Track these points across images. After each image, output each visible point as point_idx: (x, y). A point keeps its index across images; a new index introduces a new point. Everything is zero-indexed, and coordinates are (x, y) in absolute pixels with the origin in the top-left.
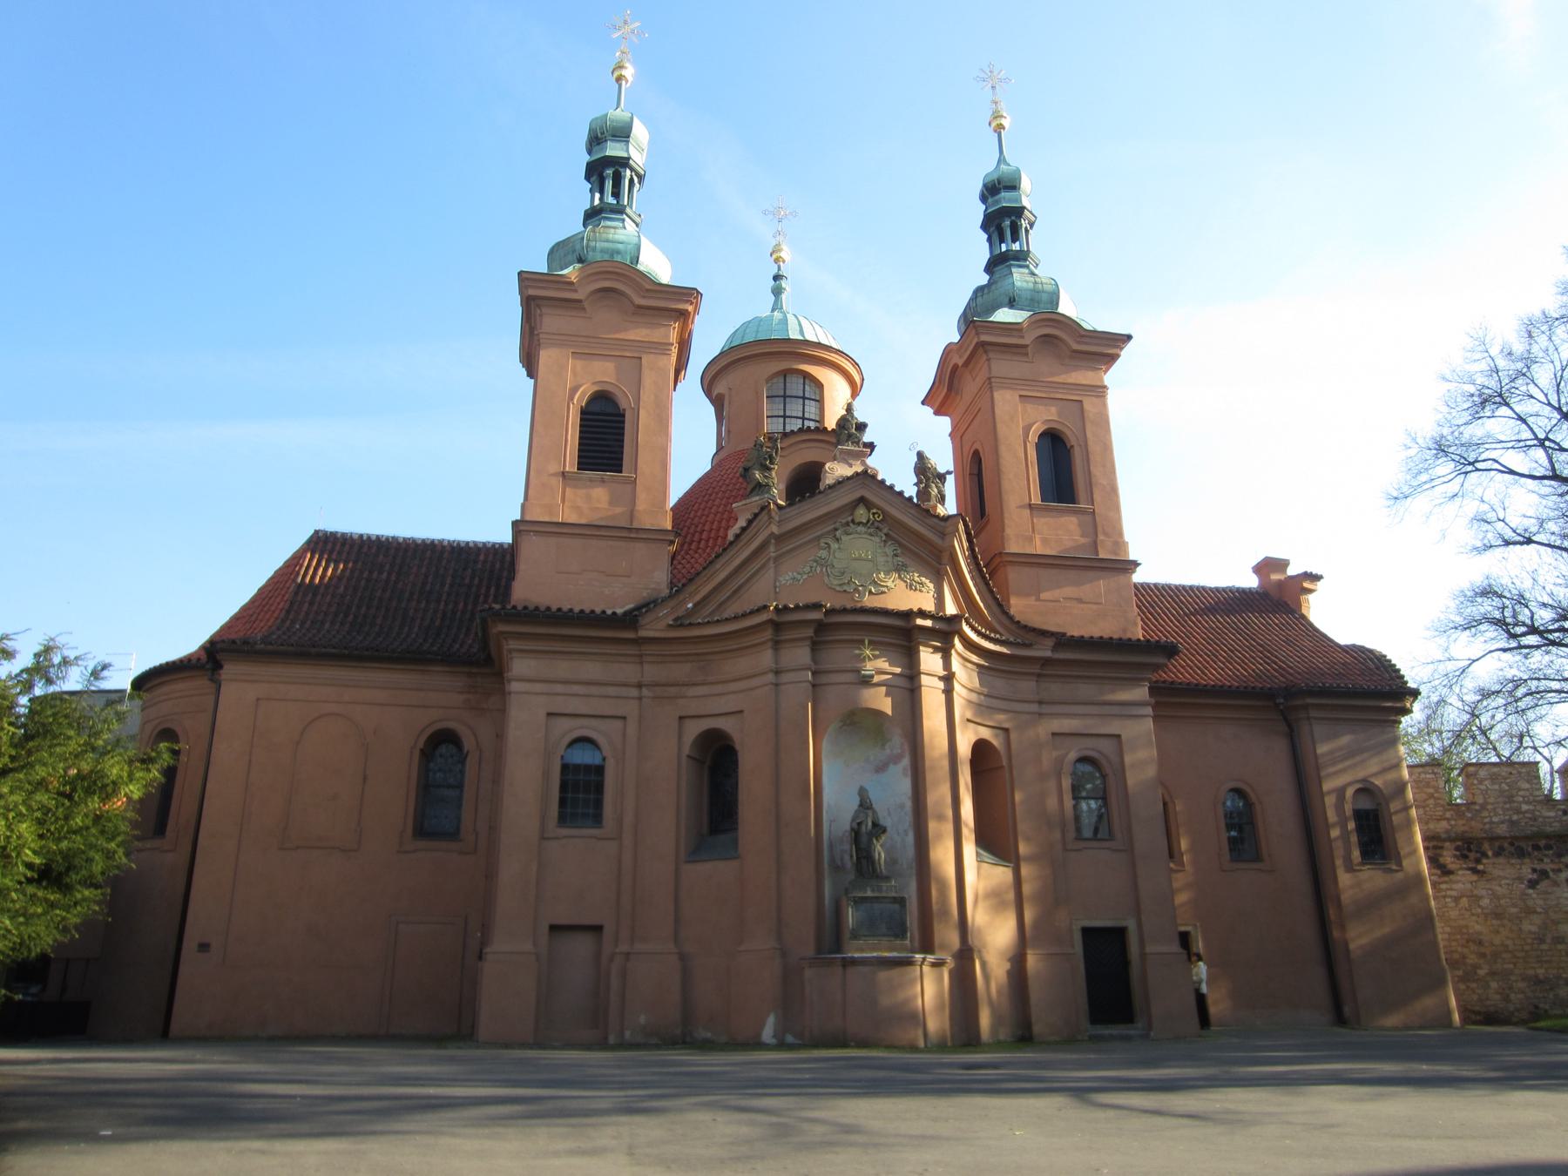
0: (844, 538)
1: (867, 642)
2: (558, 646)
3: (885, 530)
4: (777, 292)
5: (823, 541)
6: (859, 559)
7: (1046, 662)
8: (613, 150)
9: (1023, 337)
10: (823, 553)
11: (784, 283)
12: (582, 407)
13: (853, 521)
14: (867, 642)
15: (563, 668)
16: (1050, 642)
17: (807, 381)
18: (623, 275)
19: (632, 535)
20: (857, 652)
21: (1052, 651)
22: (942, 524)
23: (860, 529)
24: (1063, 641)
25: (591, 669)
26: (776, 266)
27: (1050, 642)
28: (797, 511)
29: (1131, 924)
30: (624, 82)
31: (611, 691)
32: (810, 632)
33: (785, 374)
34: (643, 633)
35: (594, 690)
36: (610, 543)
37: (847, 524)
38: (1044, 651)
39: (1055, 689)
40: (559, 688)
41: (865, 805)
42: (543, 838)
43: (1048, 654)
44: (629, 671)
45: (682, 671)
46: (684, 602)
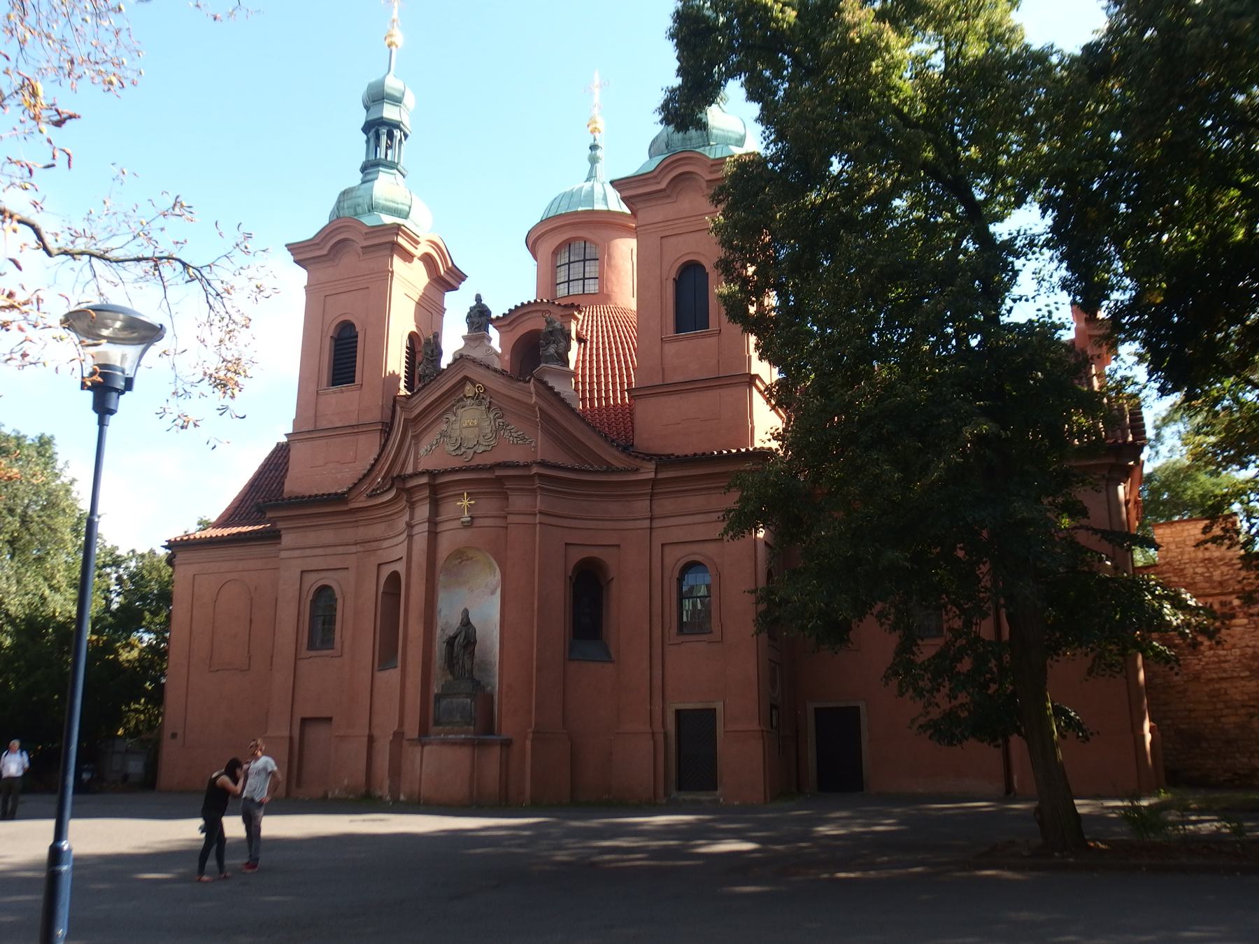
0: (460, 411)
1: (465, 495)
2: (307, 523)
3: (488, 400)
4: (593, 160)
5: (445, 416)
6: (468, 427)
7: (654, 482)
8: (389, 112)
9: (658, 183)
10: (444, 427)
11: (599, 153)
12: (331, 337)
13: (465, 396)
14: (465, 495)
15: (312, 537)
16: (652, 466)
17: (588, 245)
18: (342, 227)
19: (355, 431)
20: (459, 503)
21: (656, 473)
22: (526, 385)
23: (469, 402)
24: (665, 461)
25: (327, 536)
26: (592, 136)
27: (652, 466)
28: (420, 398)
29: (719, 706)
30: (394, 48)
31: (340, 550)
32: (426, 493)
33: (568, 244)
34: (353, 505)
35: (329, 551)
36: (345, 438)
37: (461, 400)
38: (648, 472)
39: (666, 505)
40: (308, 552)
41: (466, 623)
42: (296, 659)
43: (652, 475)
44: (349, 534)
45: (377, 530)
46: (376, 477)
